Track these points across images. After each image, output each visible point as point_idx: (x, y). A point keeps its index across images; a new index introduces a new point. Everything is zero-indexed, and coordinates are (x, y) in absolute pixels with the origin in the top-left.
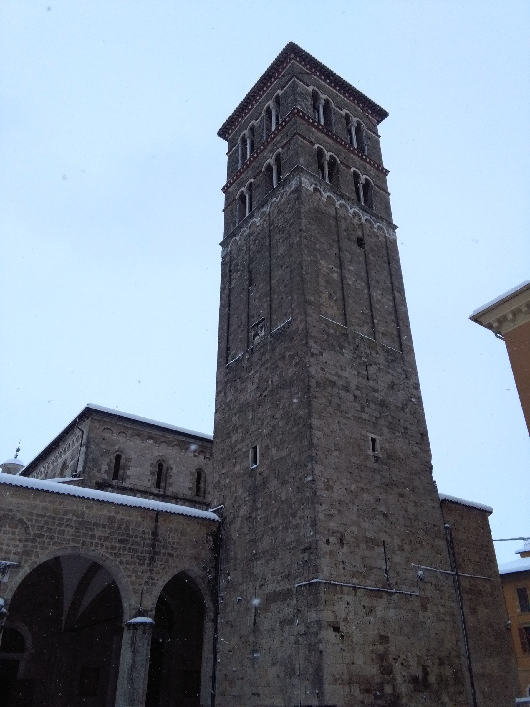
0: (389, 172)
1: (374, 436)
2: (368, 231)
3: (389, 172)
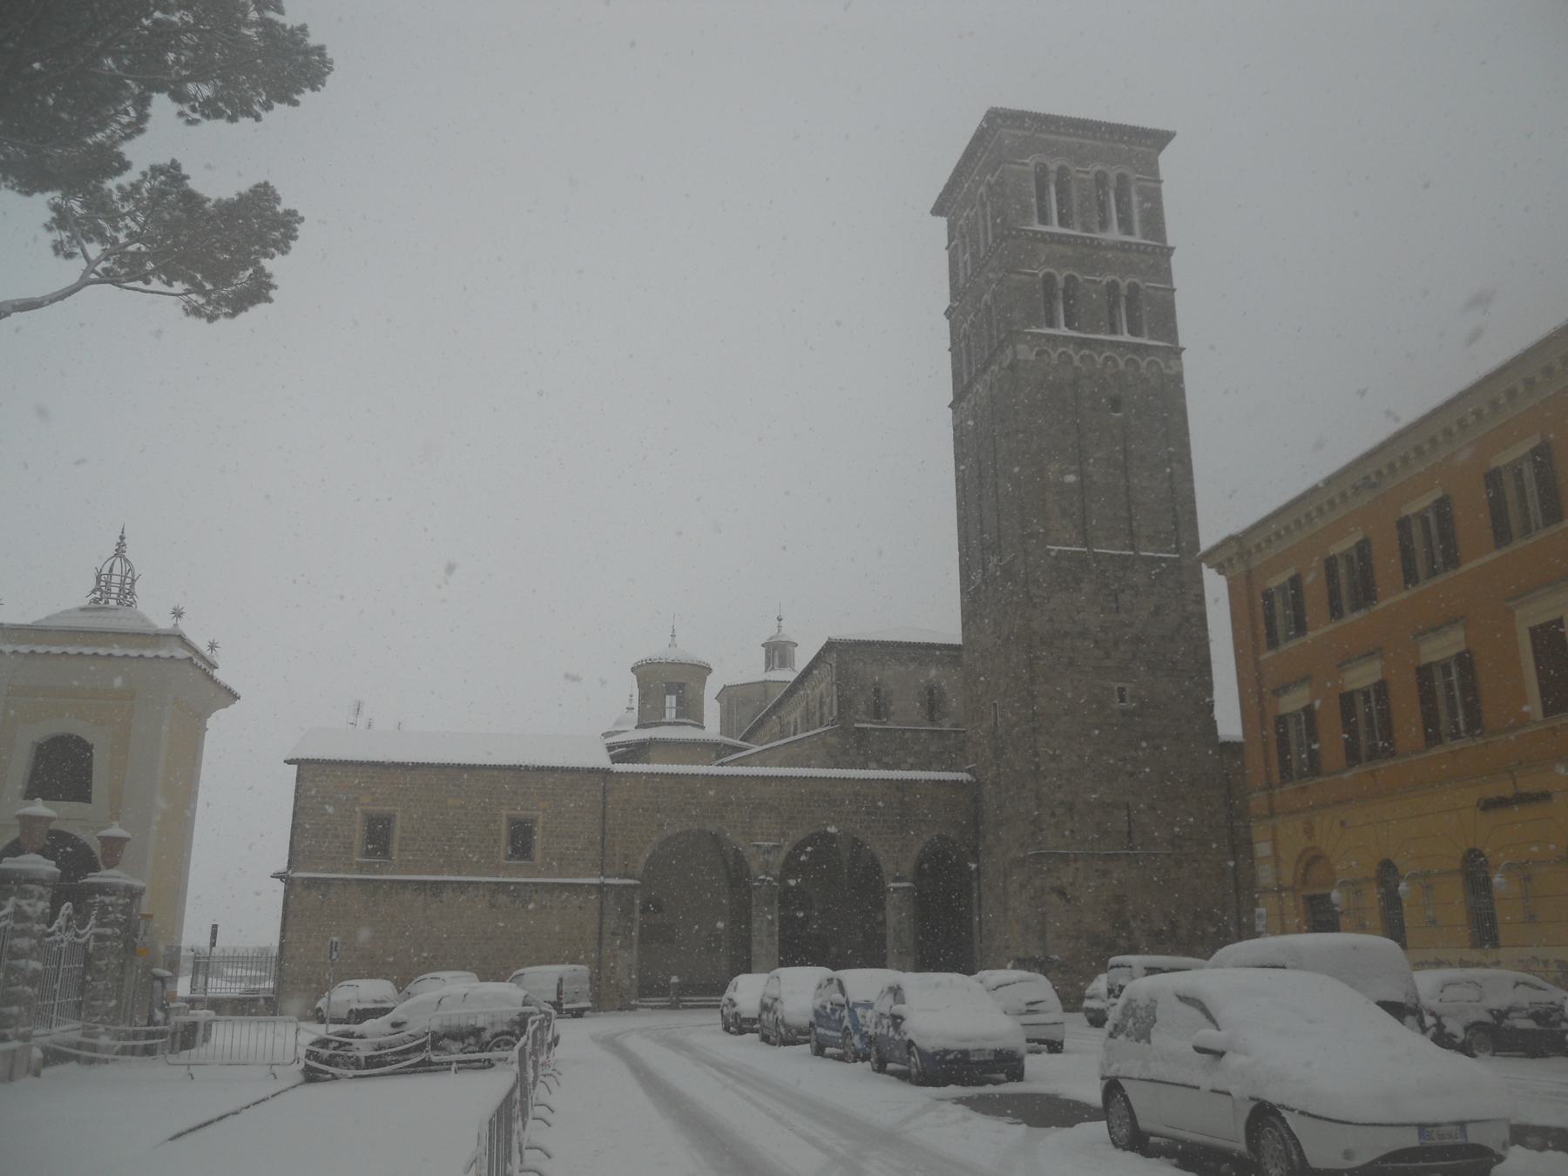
0: (1173, 249)
1: (1121, 685)
2: (1130, 378)
3: (1173, 249)
